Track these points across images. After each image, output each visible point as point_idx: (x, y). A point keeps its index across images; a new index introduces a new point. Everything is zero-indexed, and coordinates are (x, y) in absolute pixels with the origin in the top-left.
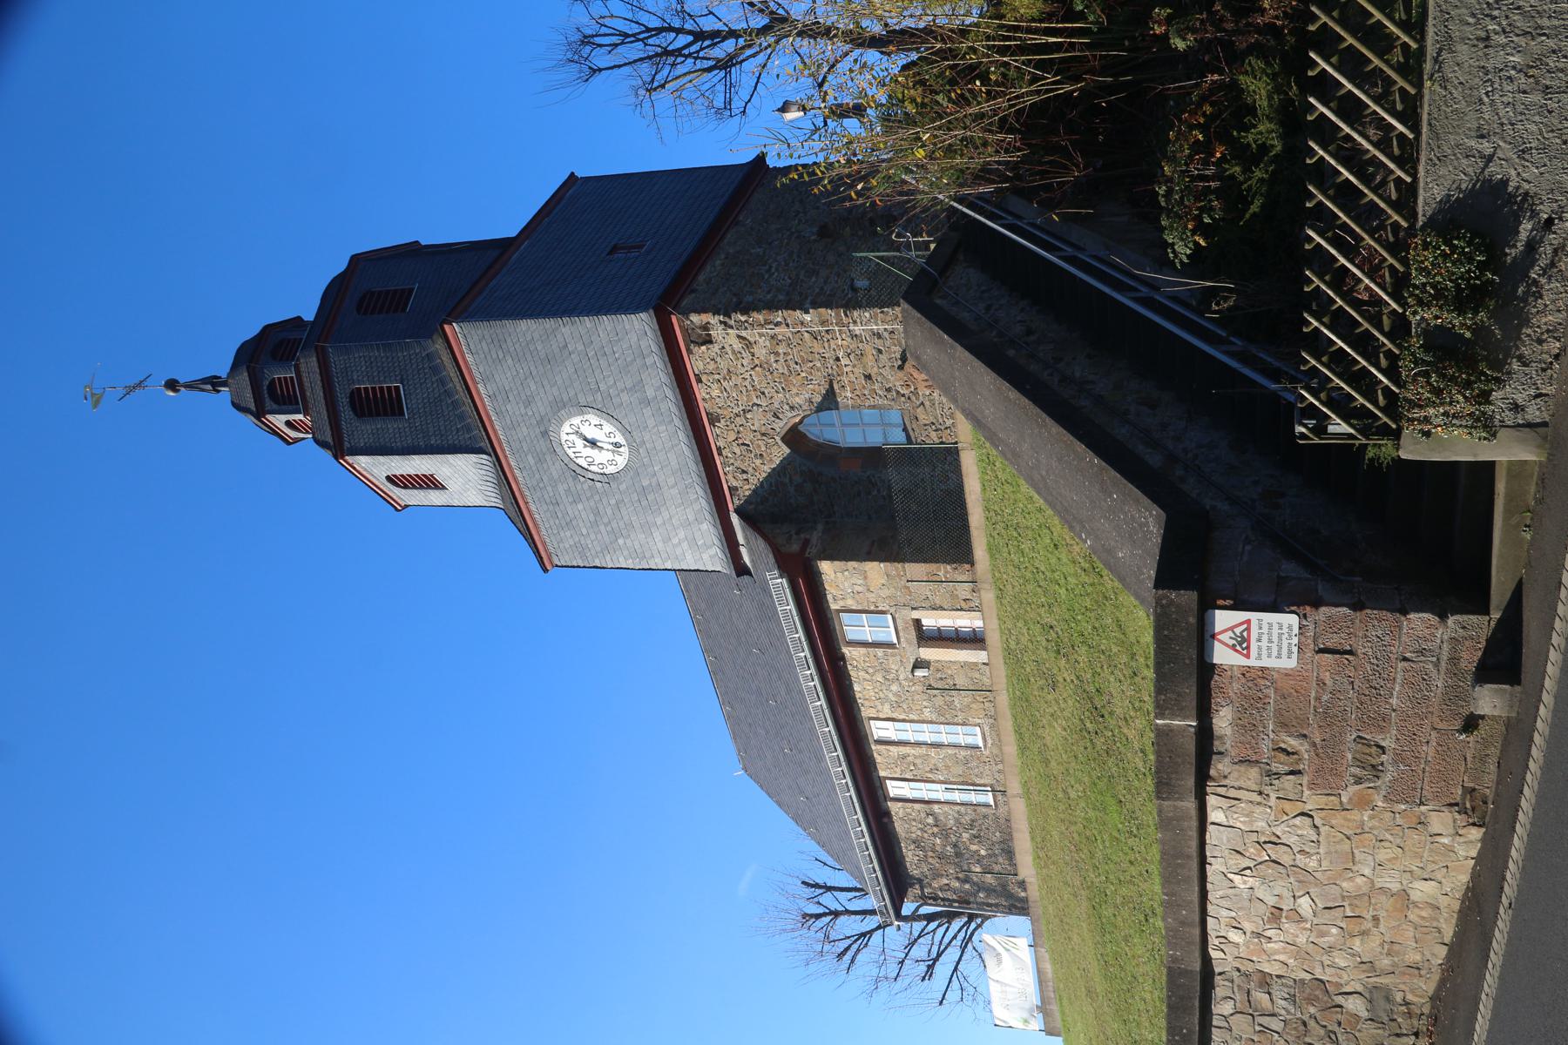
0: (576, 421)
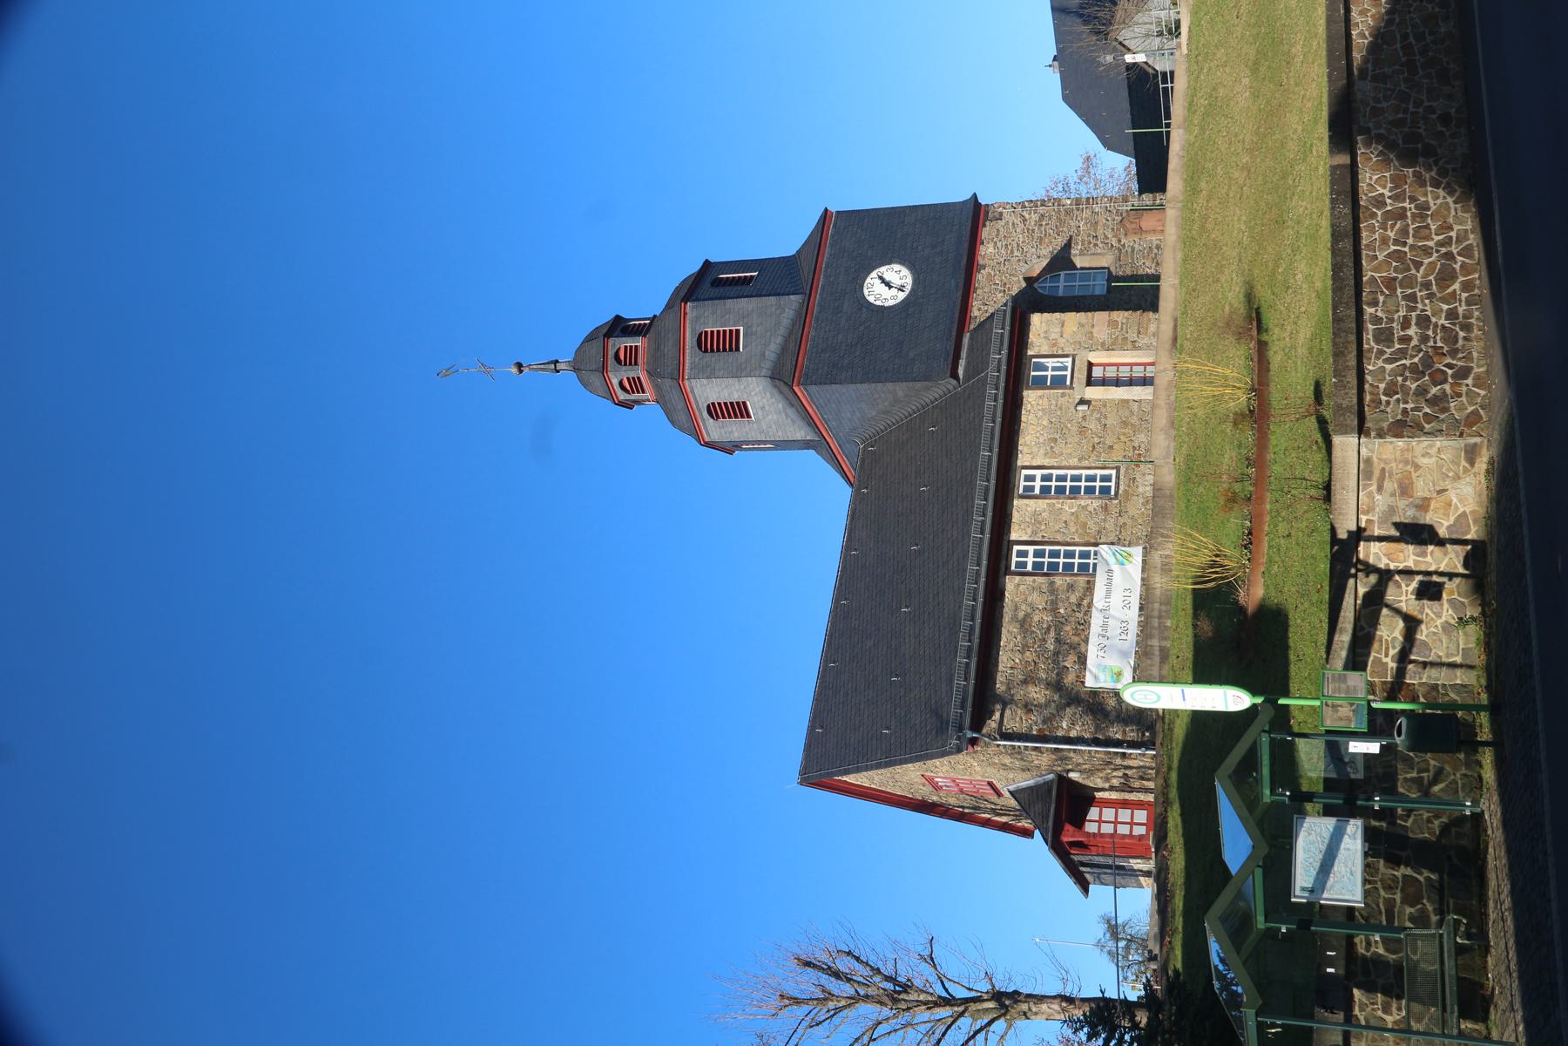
0: (883, 269)
